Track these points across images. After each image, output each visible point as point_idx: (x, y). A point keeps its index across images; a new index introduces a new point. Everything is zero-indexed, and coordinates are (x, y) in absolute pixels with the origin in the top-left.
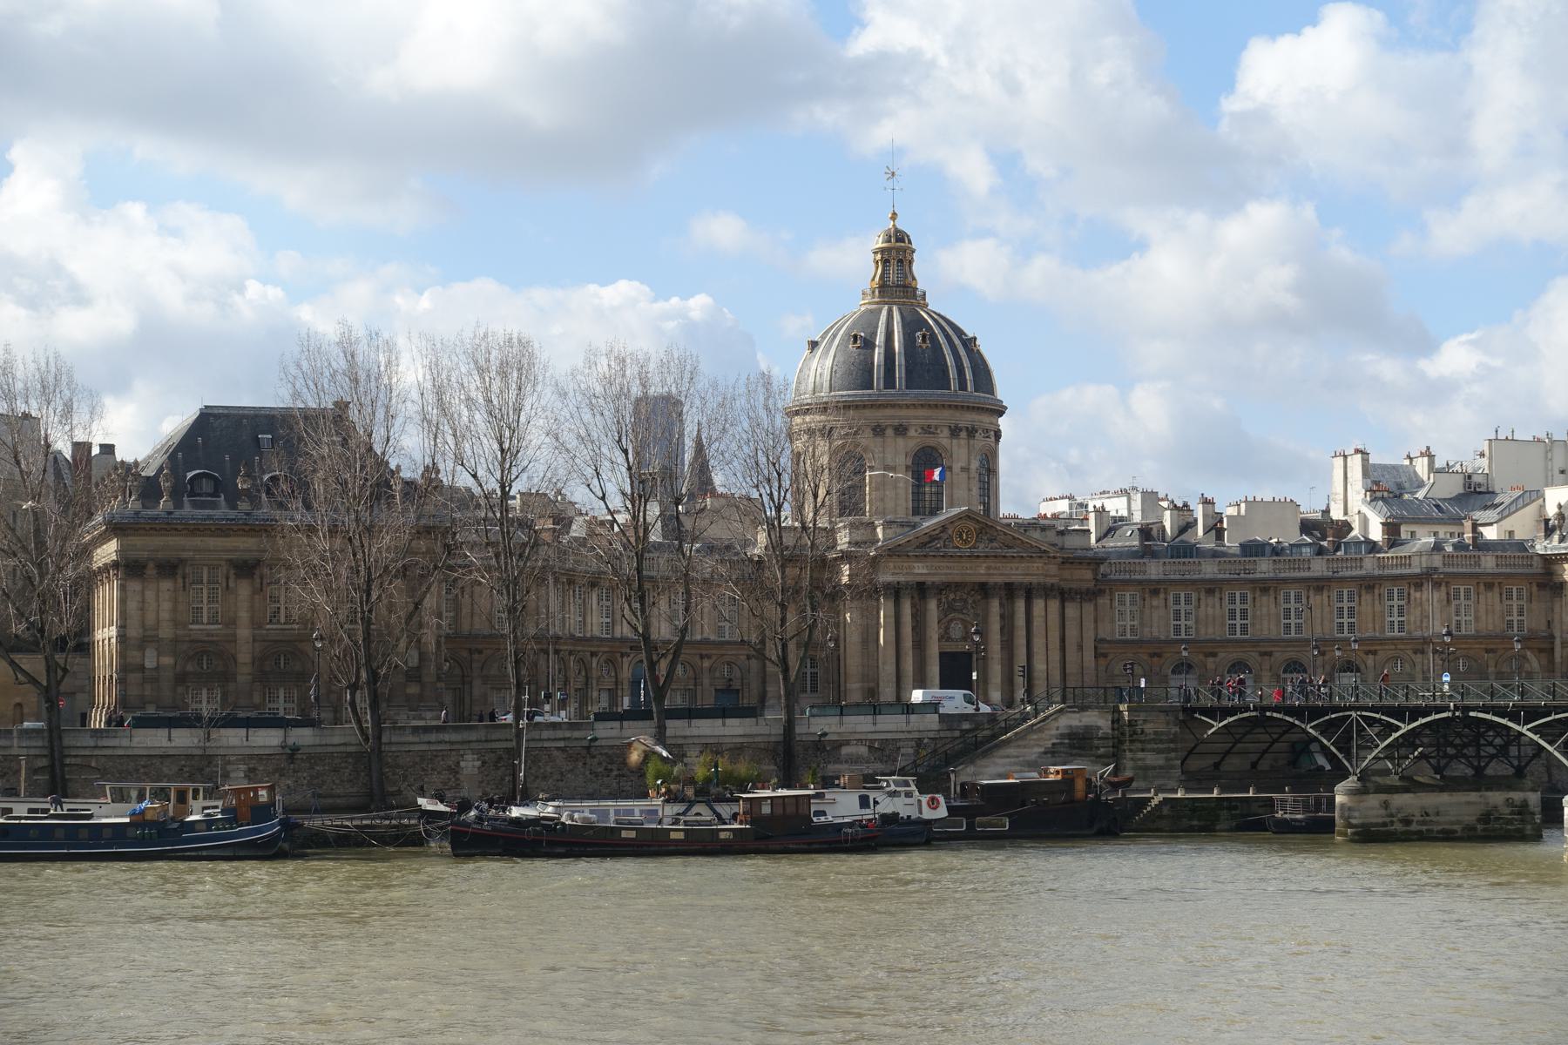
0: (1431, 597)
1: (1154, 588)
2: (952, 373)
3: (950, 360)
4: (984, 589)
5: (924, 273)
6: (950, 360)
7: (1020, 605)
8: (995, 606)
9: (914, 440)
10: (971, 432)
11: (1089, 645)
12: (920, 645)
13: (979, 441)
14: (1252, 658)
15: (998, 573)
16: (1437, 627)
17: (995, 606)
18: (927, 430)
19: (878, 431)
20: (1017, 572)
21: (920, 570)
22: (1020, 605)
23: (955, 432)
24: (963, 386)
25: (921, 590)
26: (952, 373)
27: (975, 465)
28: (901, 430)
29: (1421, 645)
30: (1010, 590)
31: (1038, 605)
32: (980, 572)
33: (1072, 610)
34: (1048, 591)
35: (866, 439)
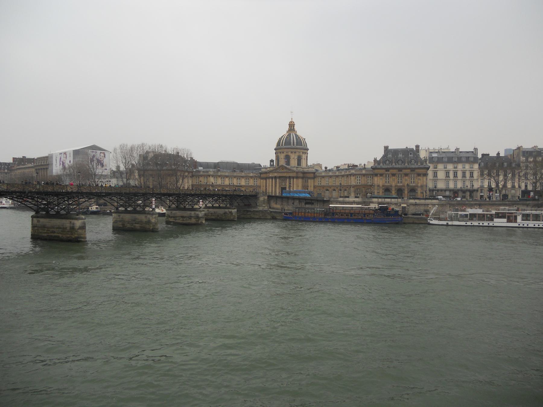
0: (352, 178)
1: (323, 177)
2: (292, 143)
3: (292, 141)
4: (286, 177)
5: (296, 128)
6: (292, 141)
7: (292, 180)
8: (288, 180)
9: (285, 154)
10: (295, 152)
11: (312, 186)
12: (276, 186)
13: (297, 154)
14: (335, 188)
15: (288, 175)
16: (353, 183)
17: (288, 180)
18: (287, 152)
19: (280, 153)
20: (291, 175)
21: (276, 174)
22: (292, 180)
23: (292, 152)
24: (294, 145)
25: (276, 178)
26: (292, 143)
27: (296, 157)
28: (283, 153)
29: (351, 186)
30: (290, 177)
31: (295, 180)
32: (285, 175)
33: (309, 181)
34: (297, 178)
35: (279, 154)
